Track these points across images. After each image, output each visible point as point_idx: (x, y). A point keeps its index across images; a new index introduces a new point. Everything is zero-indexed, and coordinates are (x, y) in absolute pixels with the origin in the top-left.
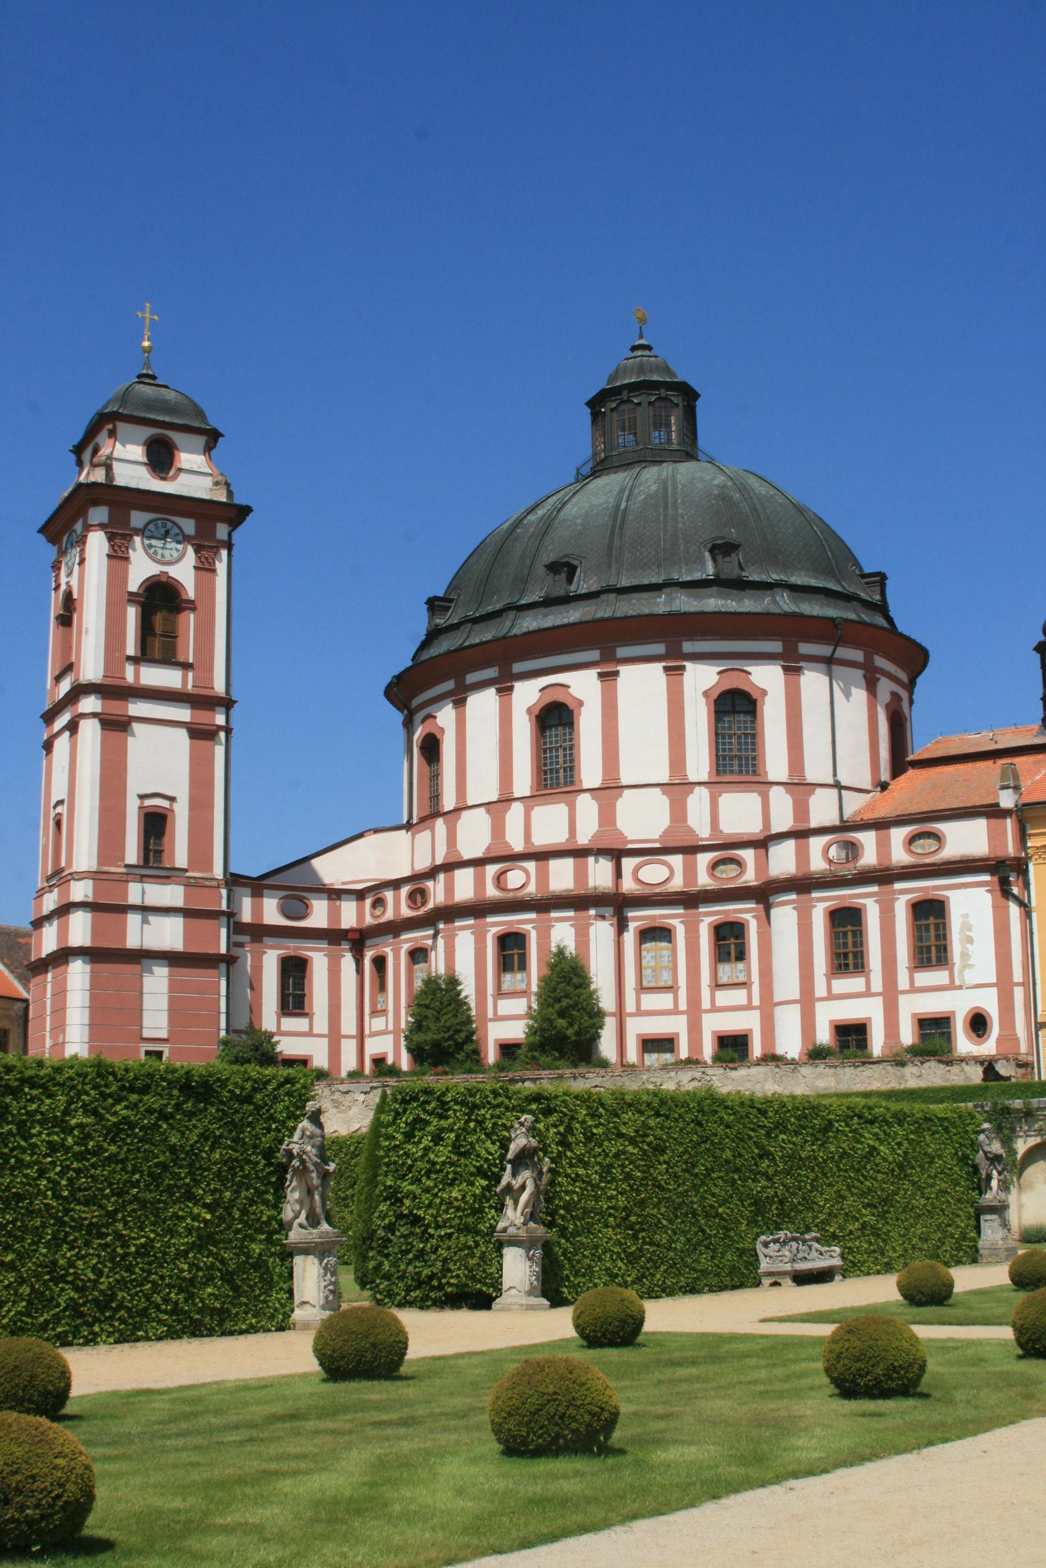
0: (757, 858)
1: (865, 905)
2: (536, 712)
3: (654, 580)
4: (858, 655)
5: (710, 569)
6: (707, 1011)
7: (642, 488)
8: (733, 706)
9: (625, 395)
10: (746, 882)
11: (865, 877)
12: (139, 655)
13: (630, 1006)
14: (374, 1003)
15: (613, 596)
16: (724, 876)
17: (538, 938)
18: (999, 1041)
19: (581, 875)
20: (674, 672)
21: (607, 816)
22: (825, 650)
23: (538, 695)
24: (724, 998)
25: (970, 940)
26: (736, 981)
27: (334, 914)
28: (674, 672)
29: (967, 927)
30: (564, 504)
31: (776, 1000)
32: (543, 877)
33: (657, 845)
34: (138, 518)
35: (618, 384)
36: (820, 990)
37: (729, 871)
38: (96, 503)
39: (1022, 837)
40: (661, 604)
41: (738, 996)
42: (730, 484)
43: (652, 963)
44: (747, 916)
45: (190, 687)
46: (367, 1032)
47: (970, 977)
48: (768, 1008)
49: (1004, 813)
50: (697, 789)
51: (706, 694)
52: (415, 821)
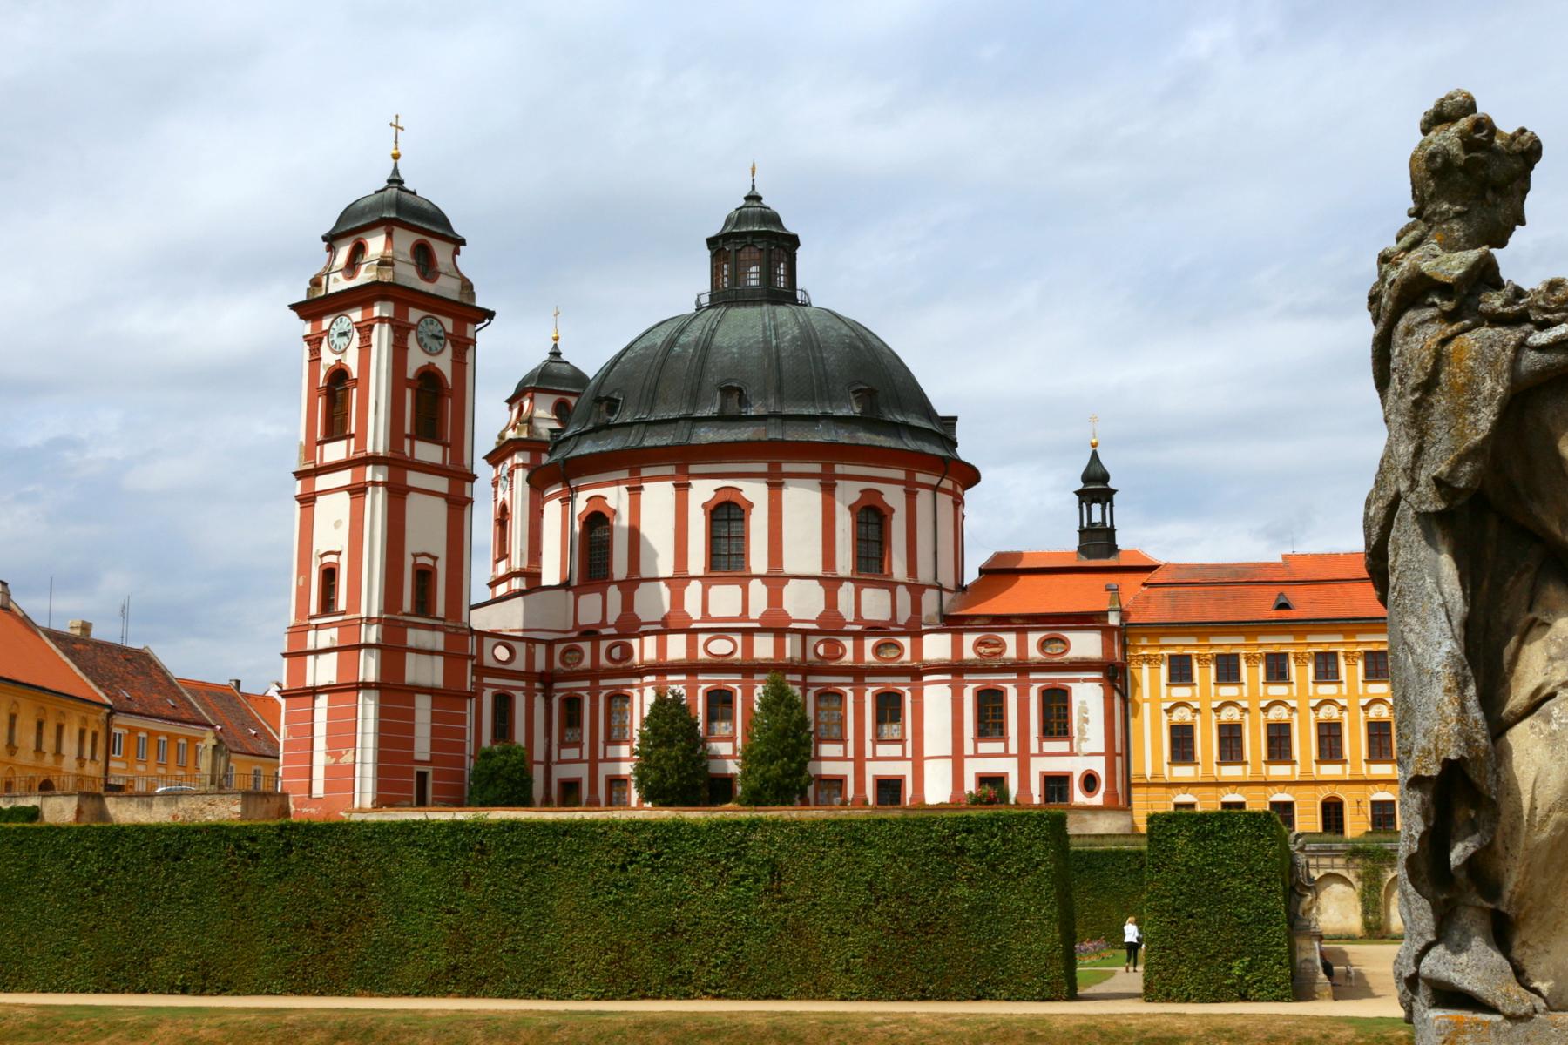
0: (913, 645)
1: (1006, 689)
2: (711, 507)
3: (812, 411)
5: (853, 410)
7: (784, 329)
9: (749, 240)
10: (903, 662)
11: (1005, 669)
12: (414, 433)
15: (779, 421)
17: (743, 695)
18: (1105, 795)
19: (779, 649)
21: (775, 599)
22: (934, 480)
23: (712, 494)
24: (883, 750)
25: (1086, 720)
27: (530, 657)
28: (828, 489)
30: (714, 331)
31: (926, 754)
32: (748, 647)
33: (814, 626)
34: (414, 315)
35: (744, 230)
36: (969, 749)
37: (891, 653)
38: (383, 298)
39: (1125, 648)
40: (820, 434)
41: (895, 750)
42: (853, 334)
43: (826, 720)
44: (904, 689)
46: (555, 758)
47: (1086, 747)
48: (918, 760)
49: (1113, 628)
50: (845, 584)
52: (575, 582)
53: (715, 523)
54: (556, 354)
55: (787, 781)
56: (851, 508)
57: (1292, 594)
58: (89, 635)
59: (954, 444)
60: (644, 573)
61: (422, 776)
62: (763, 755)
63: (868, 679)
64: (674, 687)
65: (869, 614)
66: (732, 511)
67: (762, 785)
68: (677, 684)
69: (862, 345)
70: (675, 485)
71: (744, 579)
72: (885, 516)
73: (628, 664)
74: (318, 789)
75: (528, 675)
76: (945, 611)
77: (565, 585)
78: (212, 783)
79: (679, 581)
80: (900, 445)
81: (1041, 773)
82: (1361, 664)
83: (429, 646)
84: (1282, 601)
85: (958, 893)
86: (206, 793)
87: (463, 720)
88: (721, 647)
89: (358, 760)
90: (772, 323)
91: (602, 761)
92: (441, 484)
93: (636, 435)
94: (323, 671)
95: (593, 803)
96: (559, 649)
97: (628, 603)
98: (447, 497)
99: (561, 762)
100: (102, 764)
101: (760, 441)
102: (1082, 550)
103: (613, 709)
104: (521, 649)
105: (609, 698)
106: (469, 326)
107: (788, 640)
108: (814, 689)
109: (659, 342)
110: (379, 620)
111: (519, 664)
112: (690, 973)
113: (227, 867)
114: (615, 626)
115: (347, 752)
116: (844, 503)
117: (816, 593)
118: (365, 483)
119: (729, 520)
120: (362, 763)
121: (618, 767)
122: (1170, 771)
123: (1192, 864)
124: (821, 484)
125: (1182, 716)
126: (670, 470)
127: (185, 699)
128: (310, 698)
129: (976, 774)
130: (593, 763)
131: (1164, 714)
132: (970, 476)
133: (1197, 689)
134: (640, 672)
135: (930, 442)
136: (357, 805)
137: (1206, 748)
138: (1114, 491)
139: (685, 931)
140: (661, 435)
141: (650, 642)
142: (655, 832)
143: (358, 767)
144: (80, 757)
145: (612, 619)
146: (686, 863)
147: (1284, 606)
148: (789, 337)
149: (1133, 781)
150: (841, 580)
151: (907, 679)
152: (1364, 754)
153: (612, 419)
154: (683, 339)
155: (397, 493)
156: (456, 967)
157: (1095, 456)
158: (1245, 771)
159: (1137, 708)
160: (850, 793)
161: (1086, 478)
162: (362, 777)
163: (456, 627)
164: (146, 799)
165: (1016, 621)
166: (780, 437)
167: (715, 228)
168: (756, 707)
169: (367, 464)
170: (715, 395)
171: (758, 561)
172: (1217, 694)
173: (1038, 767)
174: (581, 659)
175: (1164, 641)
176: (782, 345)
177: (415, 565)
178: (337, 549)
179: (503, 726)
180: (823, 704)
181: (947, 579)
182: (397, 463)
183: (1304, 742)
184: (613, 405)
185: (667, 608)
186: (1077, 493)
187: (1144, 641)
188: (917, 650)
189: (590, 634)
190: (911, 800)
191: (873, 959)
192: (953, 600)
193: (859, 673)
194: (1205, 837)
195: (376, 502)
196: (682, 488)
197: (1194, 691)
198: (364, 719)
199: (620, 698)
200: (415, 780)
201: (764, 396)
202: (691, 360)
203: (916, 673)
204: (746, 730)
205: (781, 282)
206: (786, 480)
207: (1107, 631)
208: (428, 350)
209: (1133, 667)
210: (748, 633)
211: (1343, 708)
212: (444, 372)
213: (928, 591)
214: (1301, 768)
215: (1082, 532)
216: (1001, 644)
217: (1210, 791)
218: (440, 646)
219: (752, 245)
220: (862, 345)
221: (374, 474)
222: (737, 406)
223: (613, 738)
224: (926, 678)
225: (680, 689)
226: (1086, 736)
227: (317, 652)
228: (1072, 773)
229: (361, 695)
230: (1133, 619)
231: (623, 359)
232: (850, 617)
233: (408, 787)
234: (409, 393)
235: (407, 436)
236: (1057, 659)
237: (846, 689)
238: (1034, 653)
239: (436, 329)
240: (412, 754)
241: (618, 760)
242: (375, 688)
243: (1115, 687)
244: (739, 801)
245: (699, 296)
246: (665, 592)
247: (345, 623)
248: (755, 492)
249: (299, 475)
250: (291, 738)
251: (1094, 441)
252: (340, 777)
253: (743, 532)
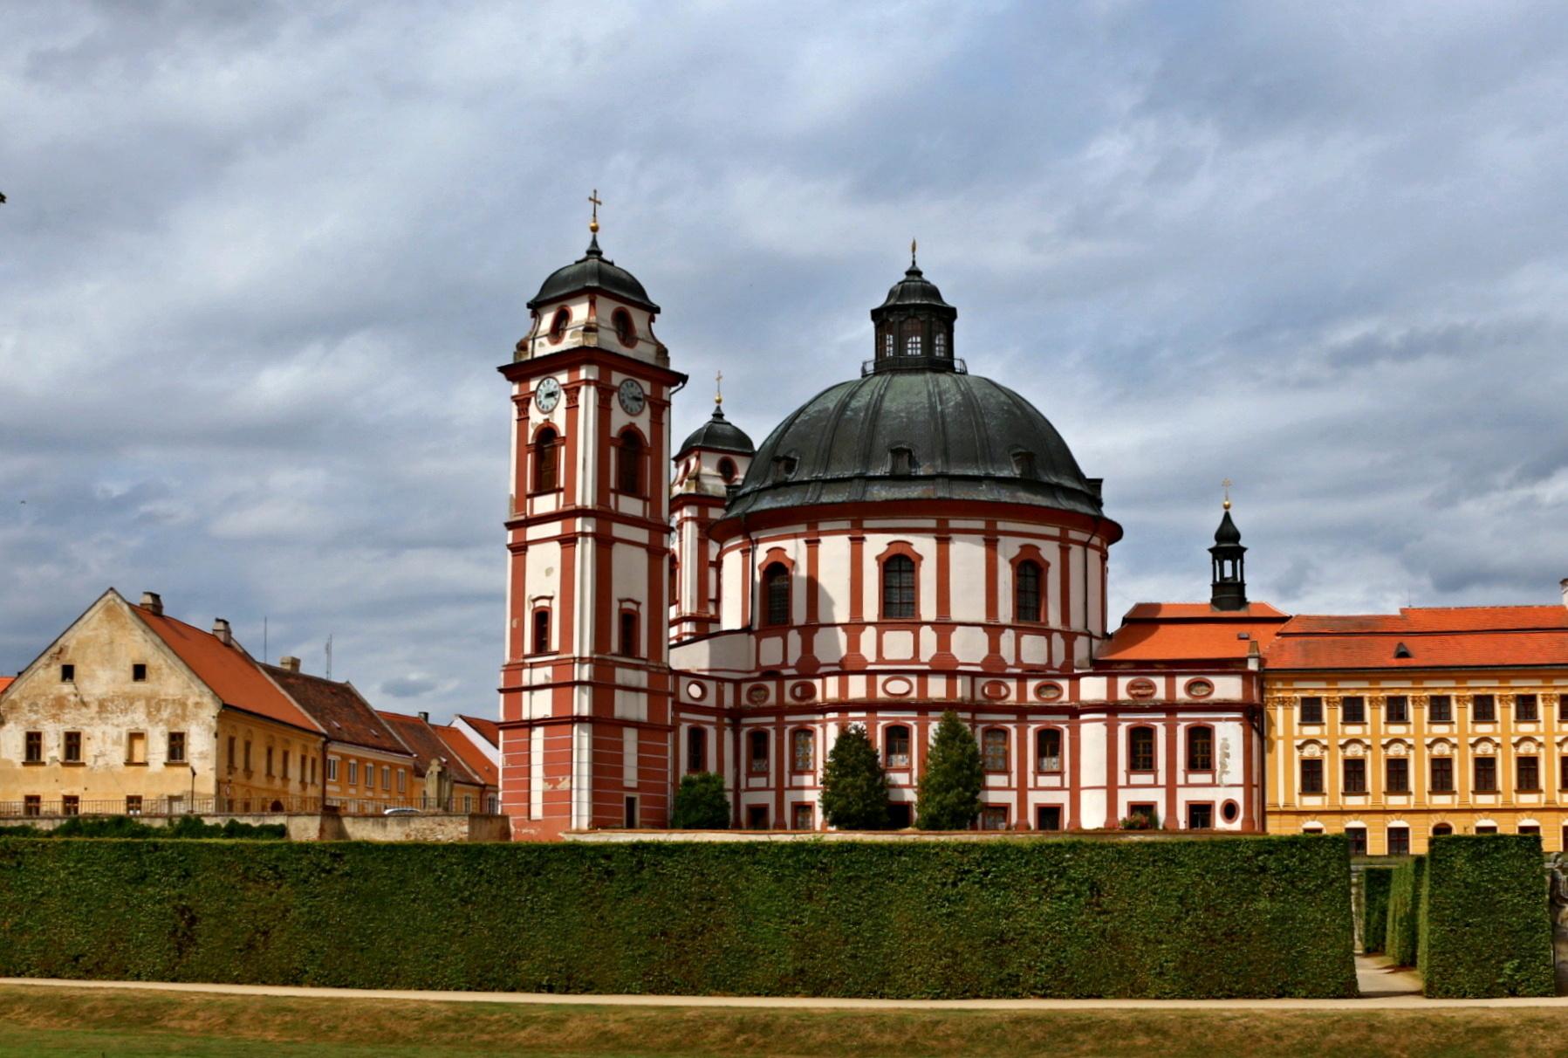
1: (1156, 727)
2: (884, 559)
3: (976, 472)
5: (1015, 472)
6: (1030, 789)
7: (948, 396)
9: (912, 312)
14: (749, 766)
15: (947, 480)
18: (1243, 821)
19: (951, 689)
21: (944, 644)
22: (1084, 537)
23: (886, 547)
24: (1044, 781)
25: (1227, 755)
27: (720, 695)
28: (991, 545)
29: (1226, 746)
30: (882, 397)
32: (923, 688)
33: (979, 669)
35: (907, 302)
36: (1122, 780)
37: (1051, 694)
39: (1262, 691)
40: (984, 494)
41: (1054, 781)
43: (992, 753)
44: (1063, 726)
46: (743, 786)
48: (1075, 790)
49: (1252, 673)
50: (1007, 631)
52: (756, 627)
53: (889, 574)
54: (718, 415)
55: (962, 808)
56: (1012, 561)
57: (1410, 643)
58: (298, 670)
59: (1098, 503)
60: (822, 619)
61: (631, 801)
62: (940, 784)
63: (1030, 717)
64: (857, 723)
65: (1027, 658)
66: (903, 563)
67: (939, 812)
68: (857, 720)
69: (1019, 412)
70: (851, 539)
71: (915, 625)
73: (811, 702)
74: (537, 812)
75: (718, 711)
76: (1094, 657)
77: (747, 629)
78: (439, 806)
79: (855, 626)
80: (1056, 505)
81: (1187, 802)
82: (1470, 707)
83: (634, 683)
84: (1402, 650)
85: (1261, 906)
86: (435, 815)
87: (664, 751)
88: (898, 687)
89: (574, 786)
90: (936, 390)
91: (787, 789)
92: (642, 535)
93: (813, 493)
94: (539, 705)
95: (780, 826)
96: (746, 687)
97: (807, 647)
99: (749, 789)
100: (320, 788)
101: (929, 500)
102: (1214, 602)
103: (798, 742)
104: (711, 687)
105: (794, 733)
106: (665, 389)
107: (959, 682)
108: (981, 726)
109: (831, 406)
110: (591, 660)
111: (710, 701)
112: (1018, 976)
113: (584, 882)
114: (796, 667)
115: (564, 779)
116: (1005, 556)
117: (981, 637)
118: (576, 533)
119: (900, 571)
120: (579, 789)
121: (802, 796)
122: (1301, 801)
123: (1469, 880)
124: (985, 540)
125: (1312, 752)
126: (846, 525)
127: (384, 729)
128: (527, 730)
130: (780, 791)
131: (1296, 750)
132: (1113, 532)
133: (1326, 728)
134: (823, 709)
135: (1082, 502)
136: (574, 826)
137: (1333, 781)
138: (1244, 549)
139: (1013, 940)
140: (836, 492)
141: (832, 682)
142: (983, 853)
143: (574, 793)
144: (303, 782)
145: (792, 661)
146: (1013, 880)
147: (1403, 655)
148: (952, 403)
149: (1268, 809)
150: (1003, 627)
151: (1066, 718)
152: (1471, 786)
153: (790, 476)
154: (854, 404)
155: (604, 543)
156: (802, 971)
157: (1227, 518)
158: (1366, 801)
159: (1272, 744)
160: (1014, 819)
161: (1219, 536)
162: (578, 801)
163: (656, 667)
164: (380, 820)
165: (1158, 666)
166: (947, 496)
167: (880, 301)
168: (931, 742)
169: (577, 516)
170: (887, 455)
171: (928, 611)
172: (1343, 733)
173: (1184, 796)
174: (766, 697)
175: (1297, 685)
176: (947, 411)
177: (621, 610)
178: (549, 594)
179: (697, 759)
180: (990, 740)
181: (1096, 630)
182: (603, 514)
183: (1419, 775)
184: (790, 465)
185: (844, 651)
186: (1211, 550)
187: (1279, 685)
188: (1075, 692)
189: (772, 673)
190: (1069, 825)
191: (1184, 964)
192: (1100, 647)
193: (1022, 712)
194: (1480, 856)
195: (585, 552)
196: (857, 542)
197: (1322, 731)
198: (579, 749)
199: (804, 733)
200: (624, 805)
201: (931, 458)
202: (862, 424)
203: (1074, 712)
204: (922, 763)
205: (939, 352)
206: (953, 536)
207: (1247, 676)
209: (1269, 708)
210: (922, 675)
211: (1454, 746)
212: (642, 429)
214: (1416, 798)
215: (1215, 586)
216: (1152, 686)
217: (1336, 818)
218: (644, 684)
219: (914, 317)
220: (1019, 412)
221: (583, 527)
222: (907, 467)
223: (798, 769)
224: (1083, 717)
225: (861, 724)
227: (532, 688)
228: (1214, 802)
229: (575, 728)
230: (1270, 665)
231: (797, 421)
232: (1010, 661)
233: (618, 811)
234: (613, 451)
235: (612, 491)
236: (1202, 701)
237: (1010, 726)
238: (1181, 695)
239: (635, 391)
240: (622, 782)
241: (802, 788)
242: (589, 722)
243: (1253, 726)
244: (918, 826)
245: (865, 363)
246: (842, 638)
247: (558, 662)
248: (924, 546)
249: (510, 526)
250: (510, 766)
251: (1227, 503)
252: (558, 802)
253: (913, 582)
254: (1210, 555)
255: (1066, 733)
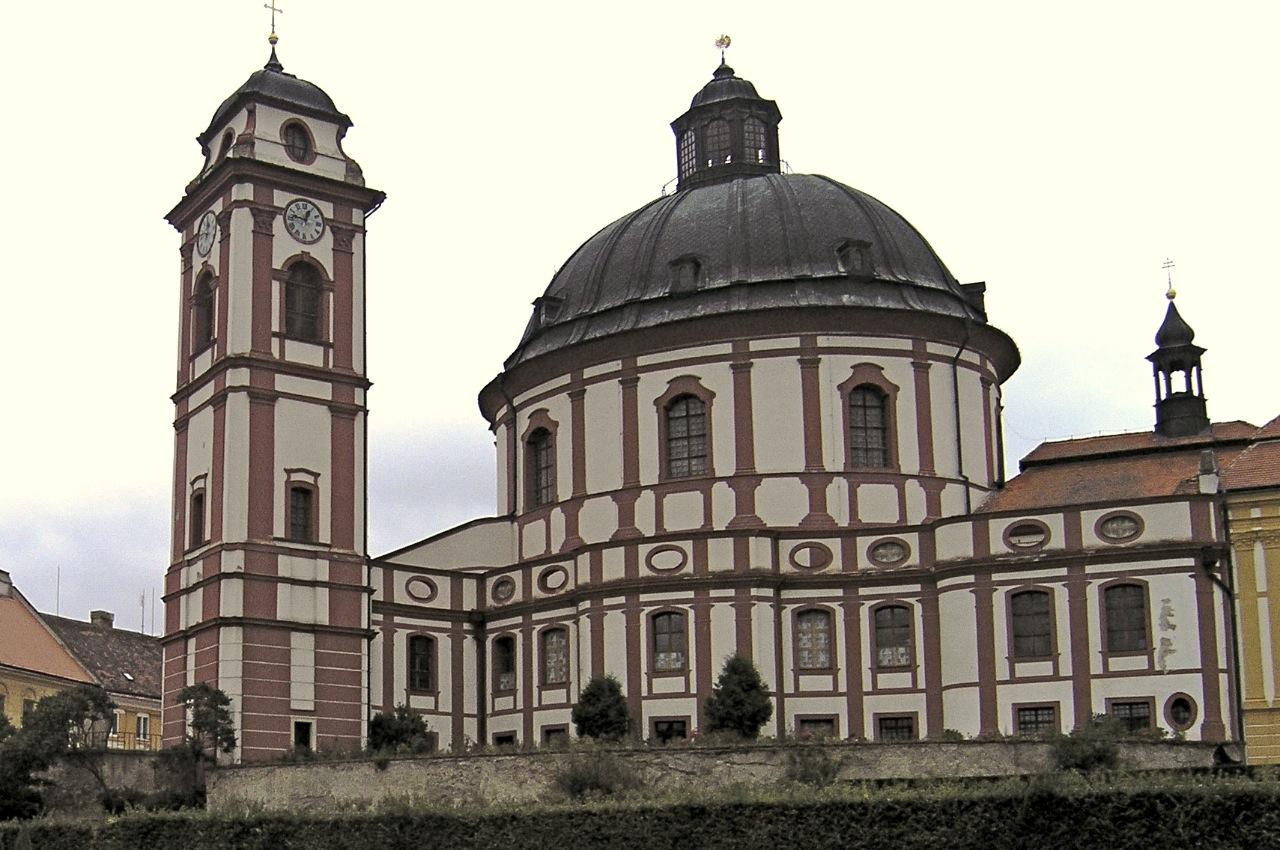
4: (975, 359)
8: (864, 399)
12: (284, 330)
13: (789, 688)
16: (885, 560)
19: (741, 554)
20: (810, 368)
21: (745, 503)
22: (952, 352)
24: (885, 680)
26: (897, 664)
28: (810, 368)
32: (701, 556)
34: (281, 198)
36: (1002, 671)
38: (241, 179)
41: (903, 680)
43: (809, 645)
45: (331, 365)
51: (840, 387)
72: (888, 396)
88: (667, 560)
92: (324, 390)
98: (332, 407)
117: (800, 491)
129: (1014, 705)
157: (1172, 309)
161: (1161, 338)
181: (978, 474)
182: (260, 363)
193: (849, 582)
208: (301, 237)
213: (949, 485)
215: (1160, 405)
226: (1172, 648)
234: (276, 286)
235: (275, 335)
237: (834, 605)
248: (717, 379)
254: (1150, 365)
255: (918, 609)
